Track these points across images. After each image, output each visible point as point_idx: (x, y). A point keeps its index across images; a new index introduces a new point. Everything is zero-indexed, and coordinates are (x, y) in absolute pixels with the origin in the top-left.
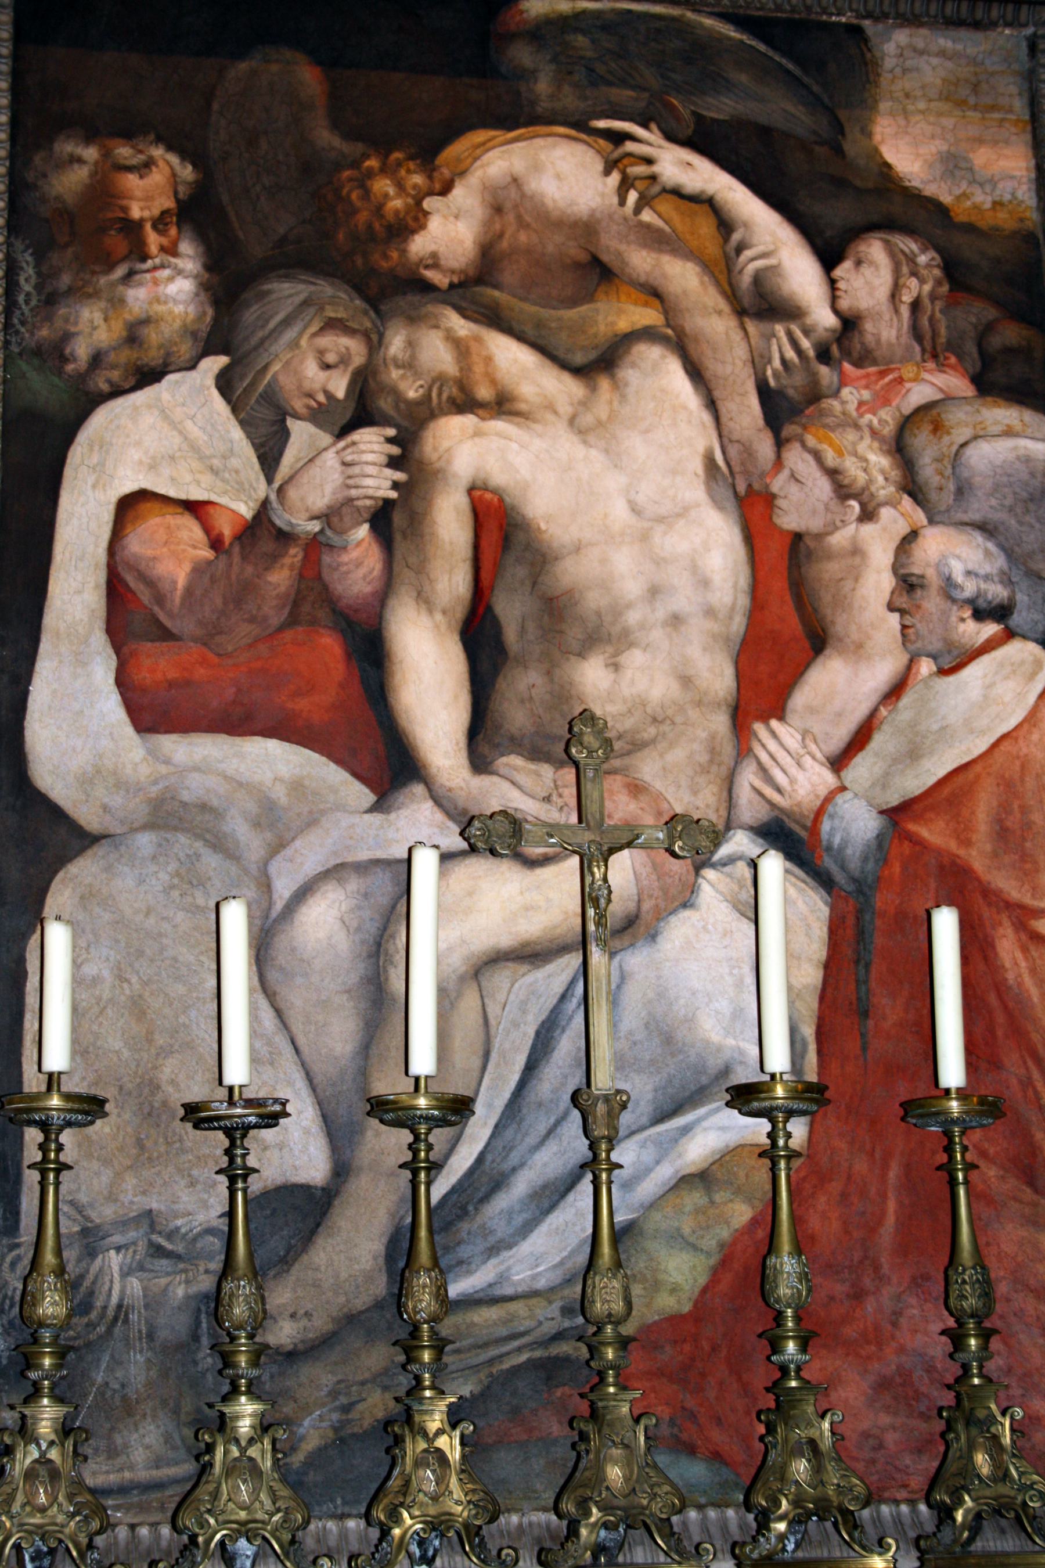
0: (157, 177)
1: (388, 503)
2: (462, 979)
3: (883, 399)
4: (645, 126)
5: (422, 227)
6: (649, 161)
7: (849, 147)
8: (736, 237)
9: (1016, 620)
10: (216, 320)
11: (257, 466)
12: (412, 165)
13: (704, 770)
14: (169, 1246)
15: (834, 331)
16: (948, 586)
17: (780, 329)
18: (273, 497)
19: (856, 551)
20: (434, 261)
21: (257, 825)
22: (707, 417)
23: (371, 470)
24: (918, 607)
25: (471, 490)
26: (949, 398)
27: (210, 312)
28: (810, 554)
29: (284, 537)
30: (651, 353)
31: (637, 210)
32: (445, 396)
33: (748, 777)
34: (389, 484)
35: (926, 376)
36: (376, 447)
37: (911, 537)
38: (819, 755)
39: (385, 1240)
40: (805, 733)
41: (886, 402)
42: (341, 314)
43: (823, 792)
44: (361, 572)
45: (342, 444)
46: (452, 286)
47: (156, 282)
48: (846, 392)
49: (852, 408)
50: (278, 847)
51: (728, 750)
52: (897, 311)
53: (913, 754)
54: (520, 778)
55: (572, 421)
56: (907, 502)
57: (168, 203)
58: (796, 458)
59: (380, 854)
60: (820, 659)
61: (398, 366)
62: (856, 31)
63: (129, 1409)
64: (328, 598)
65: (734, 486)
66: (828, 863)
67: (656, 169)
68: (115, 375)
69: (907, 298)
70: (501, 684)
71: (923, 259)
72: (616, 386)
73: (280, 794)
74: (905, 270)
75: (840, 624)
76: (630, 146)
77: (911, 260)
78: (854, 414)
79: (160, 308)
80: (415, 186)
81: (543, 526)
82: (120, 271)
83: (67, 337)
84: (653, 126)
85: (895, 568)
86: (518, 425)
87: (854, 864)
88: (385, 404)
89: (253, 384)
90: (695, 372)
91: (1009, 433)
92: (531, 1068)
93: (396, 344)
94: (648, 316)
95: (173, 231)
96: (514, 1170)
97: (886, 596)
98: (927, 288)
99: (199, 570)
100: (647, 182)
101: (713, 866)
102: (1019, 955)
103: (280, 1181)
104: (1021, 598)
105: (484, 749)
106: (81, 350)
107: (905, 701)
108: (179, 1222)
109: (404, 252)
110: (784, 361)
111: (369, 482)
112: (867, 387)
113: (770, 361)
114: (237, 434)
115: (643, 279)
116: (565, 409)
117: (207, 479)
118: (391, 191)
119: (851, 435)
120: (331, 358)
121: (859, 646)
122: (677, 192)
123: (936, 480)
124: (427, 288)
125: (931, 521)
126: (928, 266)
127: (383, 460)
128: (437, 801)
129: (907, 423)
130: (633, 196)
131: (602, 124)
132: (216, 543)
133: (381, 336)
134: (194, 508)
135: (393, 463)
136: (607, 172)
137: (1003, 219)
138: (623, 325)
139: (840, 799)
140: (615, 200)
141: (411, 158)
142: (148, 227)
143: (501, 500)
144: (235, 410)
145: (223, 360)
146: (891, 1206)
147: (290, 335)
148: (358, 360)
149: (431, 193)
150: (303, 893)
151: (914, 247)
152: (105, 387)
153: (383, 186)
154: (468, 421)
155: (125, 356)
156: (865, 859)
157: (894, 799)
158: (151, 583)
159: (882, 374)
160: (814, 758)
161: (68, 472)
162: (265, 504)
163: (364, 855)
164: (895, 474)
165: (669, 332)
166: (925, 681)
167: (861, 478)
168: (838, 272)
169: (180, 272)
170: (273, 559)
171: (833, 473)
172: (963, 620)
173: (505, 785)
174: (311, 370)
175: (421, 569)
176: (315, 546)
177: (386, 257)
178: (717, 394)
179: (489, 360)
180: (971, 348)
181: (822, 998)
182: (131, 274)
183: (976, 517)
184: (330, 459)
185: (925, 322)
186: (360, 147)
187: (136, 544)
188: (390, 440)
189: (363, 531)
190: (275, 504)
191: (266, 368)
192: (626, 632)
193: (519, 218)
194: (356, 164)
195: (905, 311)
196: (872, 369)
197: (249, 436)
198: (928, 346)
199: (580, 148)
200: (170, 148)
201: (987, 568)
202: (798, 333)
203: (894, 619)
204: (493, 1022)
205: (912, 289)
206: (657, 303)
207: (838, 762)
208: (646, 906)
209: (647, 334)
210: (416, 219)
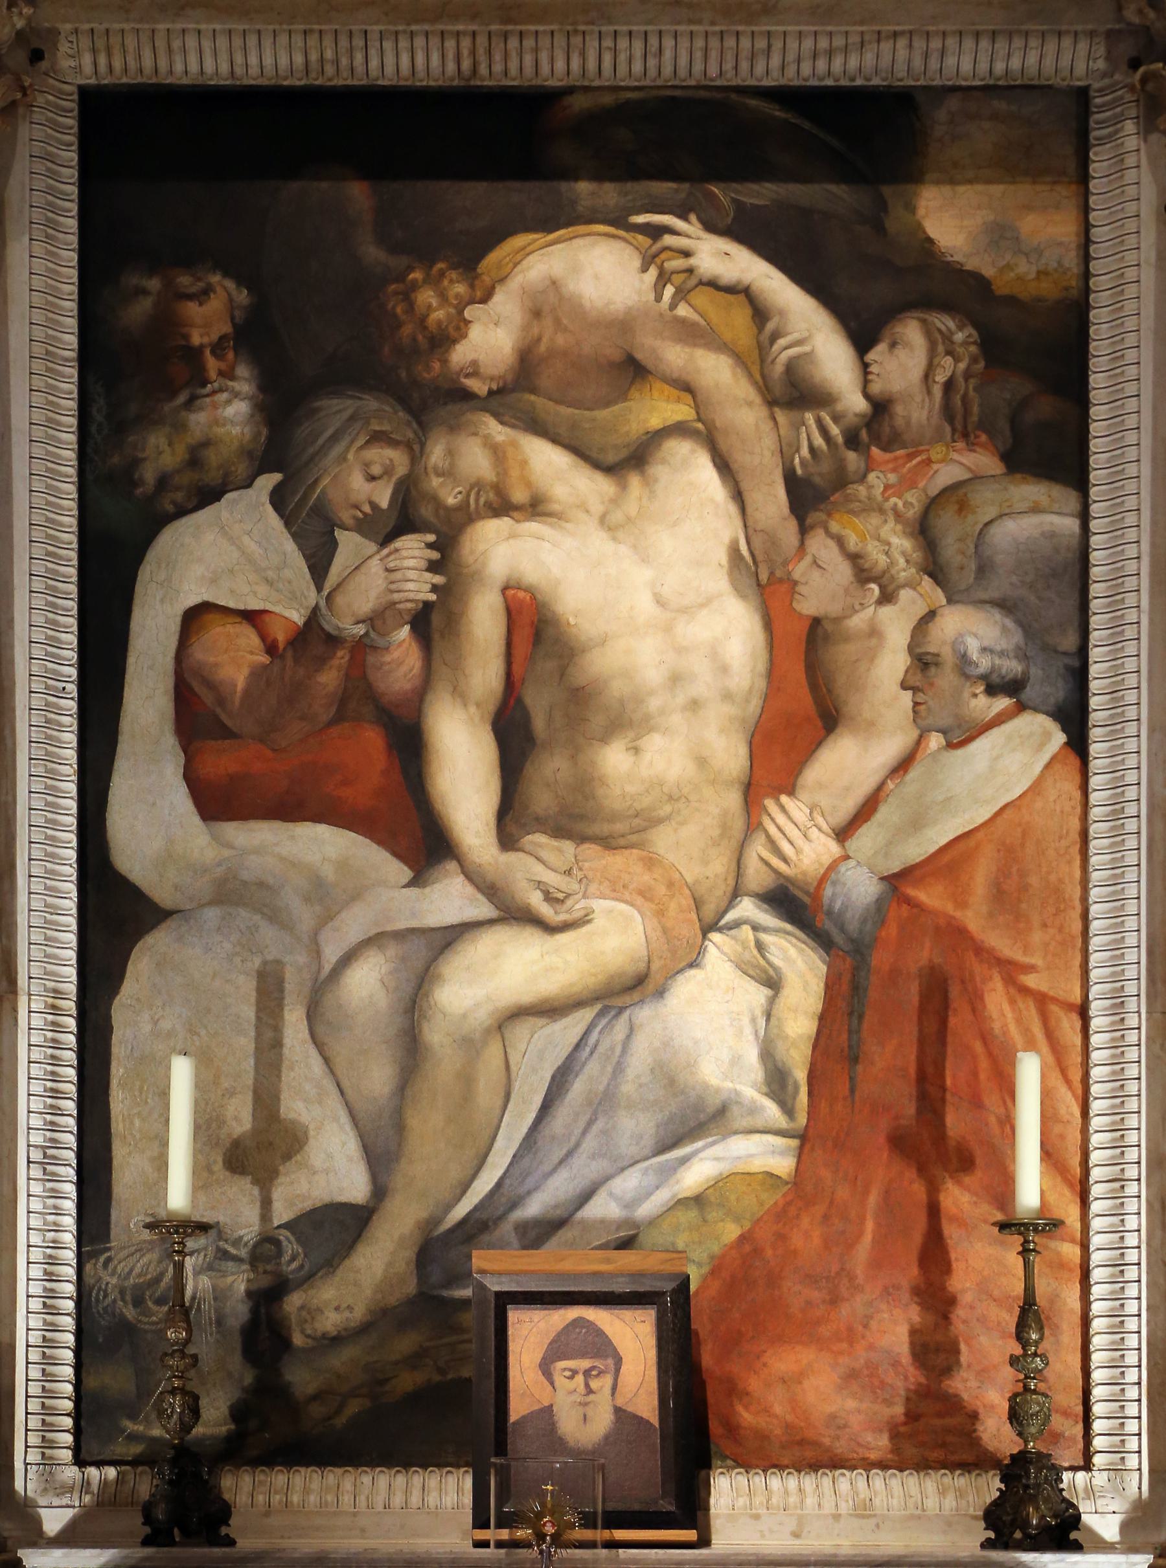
0: (216, 304)
1: (427, 606)
2: (488, 1031)
3: (909, 482)
4: (684, 217)
5: (464, 336)
6: (687, 254)
7: (891, 225)
8: (770, 326)
9: (1028, 694)
10: (270, 439)
11: (308, 576)
13: (716, 843)
14: (233, 1251)
15: (863, 416)
16: (964, 660)
17: (810, 417)
18: (323, 603)
19: (874, 632)
20: (474, 370)
21: (307, 900)
22: (733, 509)
23: (412, 574)
24: (932, 685)
25: (505, 589)
26: (977, 478)
27: (265, 432)
28: (827, 637)
29: (333, 641)
30: (680, 449)
31: (673, 306)
32: (482, 500)
33: (758, 848)
34: (428, 587)
35: (955, 456)
36: (417, 553)
37: (931, 615)
38: (825, 827)
39: (416, 1249)
41: (913, 485)
42: (386, 427)
43: (827, 861)
44: (404, 669)
45: (385, 551)
46: (491, 393)
47: (215, 406)
48: (872, 477)
50: (327, 918)
51: (739, 824)
52: (929, 392)
53: (916, 823)
54: (544, 854)
55: (603, 520)
56: (927, 581)
57: (227, 328)
58: (820, 546)
59: (414, 924)
60: (832, 737)
61: (438, 475)
64: (370, 695)
66: (828, 925)
68: (179, 496)
69: (941, 377)
70: (529, 769)
71: (959, 337)
72: (648, 482)
73: (328, 872)
74: (941, 348)
76: (668, 240)
77: (947, 338)
78: (880, 498)
79: (220, 431)
80: (457, 296)
81: (572, 621)
82: (182, 398)
83: (136, 463)
84: (693, 217)
85: (911, 648)
86: (551, 525)
87: (853, 926)
88: (426, 512)
89: (305, 497)
90: (723, 466)
91: (1036, 509)
92: (546, 1107)
93: (436, 454)
94: (681, 412)
95: (231, 355)
96: (529, 1193)
97: (901, 675)
98: (962, 366)
99: (258, 673)
100: (683, 276)
101: (720, 930)
102: (1006, 1007)
103: (327, 1199)
104: (1035, 672)
105: (512, 828)
106: (149, 474)
107: (914, 773)
108: (242, 1233)
109: (445, 362)
110: (812, 449)
111: (411, 586)
112: (894, 470)
113: (798, 450)
114: (290, 546)
115: (675, 376)
116: (597, 508)
117: (262, 589)
118: (434, 302)
119: (875, 520)
120: (376, 470)
121: (872, 724)
122: (713, 284)
123: (958, 559)
124: (467, 396)
125: (950, 601)
126: (965, 343)
127: (423, 564)
129: (933, 504)
130: (669, 291)
131: (641, 219)
132: (271, 649)
133: (423, 445)
134: (251, 617)
135: (433, 567)
136: (644, 269)
139: (843, 868)
140: (652, 296)
141: (454, 267)
142: (208, 352)
143: (533, 598)
144: (288, 524)
145: (277, 477)
146: (870, 1225)
148: (401, 470)
149: (472, 302)
150: (348, 959)
151: (951, 324)
152: (170, 508)
153: (426, 297)
154: (502, 524)
155: (186, 478)
156: (864, 921)
157: (895, 867)
159: (910, 457)
160: (820, 829)
161: (139, 589)
162: (315, 610)
163: (401, 925)
164: (917, 556)
165: (700, 426)
166: (934, 755)
167: (883, 560)
168: (871, 356)
169: (236, 395)
170: (321, 662)
171: (854, 557)
172: (975, 695)
173: (531, 860)
174: (358, 484)
175: (457, 666)
176: (362, 648)
177: (428, 368)
178: (744, 486)
179: (524, 463)
180: (1003, 424)
181: (815, 1047)
182: (193, 399)
183: (995, 594)
184: (375, 566)
186: (404, 260)
188: (430, 546)
189: (405, 632)
190: (324, 609)
191: (316, 482)
192: (647, 718)
193: (557, 322)
194: (401, 278)
195: (938, 392)
197: (301, 548)
198: (959, 427)
199: (618, 245)
200: (226, 274)
201: (1003, 644)
202: (828, 420)
204: (513, 1068)
205: (946, 367)
206: (688, 398)
207: (843, 834)
208: (655, 966)
209: (679, 430)
210: (458, 328)
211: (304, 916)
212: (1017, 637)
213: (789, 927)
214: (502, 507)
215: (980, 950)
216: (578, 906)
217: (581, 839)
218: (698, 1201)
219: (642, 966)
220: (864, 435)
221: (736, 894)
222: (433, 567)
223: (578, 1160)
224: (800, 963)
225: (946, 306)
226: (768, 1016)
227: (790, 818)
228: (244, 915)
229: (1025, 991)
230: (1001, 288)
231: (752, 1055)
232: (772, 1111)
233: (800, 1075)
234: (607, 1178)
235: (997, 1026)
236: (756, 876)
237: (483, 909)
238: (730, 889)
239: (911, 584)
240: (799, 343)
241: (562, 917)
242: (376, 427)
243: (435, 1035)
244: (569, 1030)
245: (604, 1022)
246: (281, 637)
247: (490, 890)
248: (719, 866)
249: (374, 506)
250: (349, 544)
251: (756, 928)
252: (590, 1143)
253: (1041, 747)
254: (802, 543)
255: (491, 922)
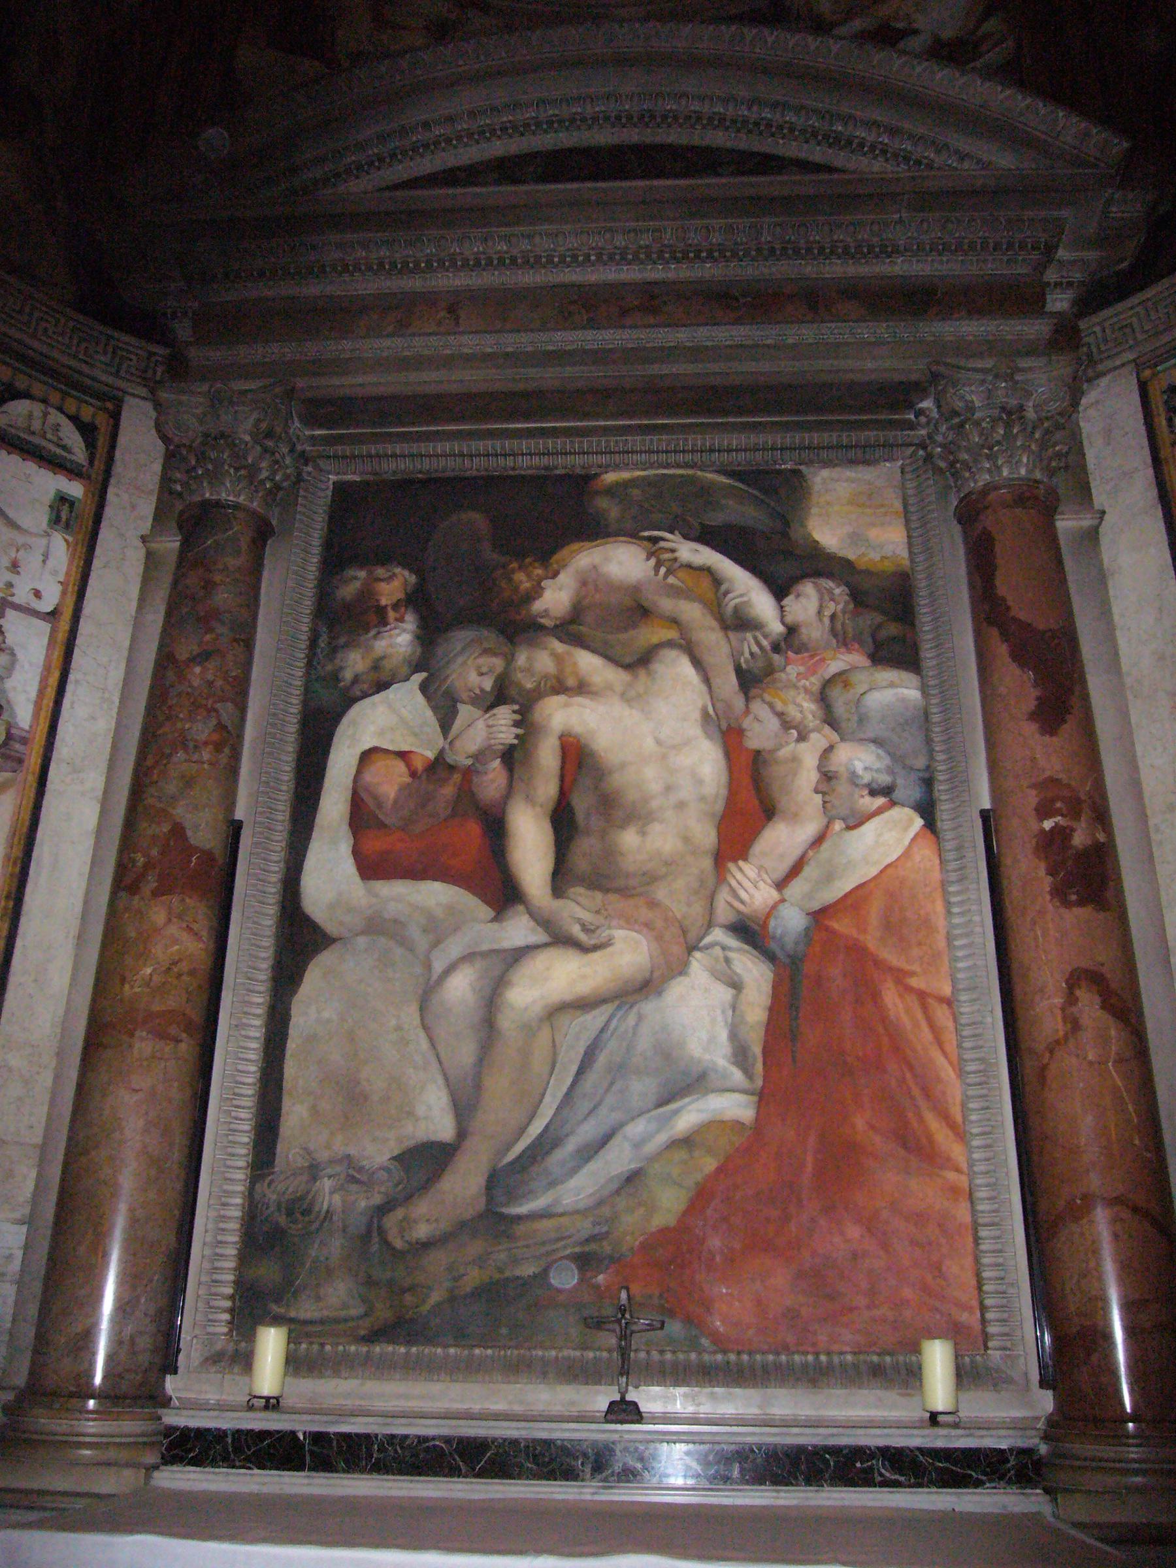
0: (396, 583)
2: (541, 1020)
3: (812, 671)
4: (672, 532)
5: (540, 596)
6: (673, 551)
7: (792, 534)
8: (723, 588)
9: (898, 794)
10: (423, 653)
11: (439, 730)
12: (536, 564)
13: (696, 892)
15: (781, 634)
16: (853, 778)
17: (749, 636)
18: (447, 747)
19: (795, 759)
22: (704, 688)
23: (504, 729)
24: (834, 790)
25: (561, 737)
26: (854, 668)
27: (419, 650)
29: (452, 768)
30: (671, 654)
31: (666, 576)
32: (549, 684)
33: (723, 896)
35: (841, 656)
36: (508, 716)
37: (830, 749)
38: (769, 881)
39: (486, 1177)
40: (761, 868)
41: (814, 673)
43: (771, 902)
46: (556, 626)
47: (391, 637)
48: (789, 668)
49: (793, 676)
50: (436, 943)
51: (711, 881)
52: (821, 620)
53: (829, 877)
54: (580, 899)
55: (622, 695)
56: (827, 729)
57: (401, 595)
58: (758, 708)
59: (496, 947)
60: (770, 824)
62: (797, 473)
63: (329, 1272)
65: (719, 726)
66: (773, 946)
67: (677, 554)
68: (365, 687)
69: (827, 613)
71: (837, 591)
72: (649, 674)
73: (439, 913)
74: (826, 597)
75: (783, 802)
76: (662, 544)
77: (830, 592)
78: (794, 680)
79: (390, 650)
82: (373, 632)
84: (676, 532)
86: (591, 700)
88: (513, 692)
90: (697, 663)
91: (892, 685)
92: (581, 1072)
93: (522, 659)
94: (671, 634)
95: (403, 609)
96: (567, 1135)
97: (813, 785)
98: (840, 607)
99: (403, 788)
101: (700, 949)
102: (898, 1001)
103: (425, 1139)
106: (348, 675)
107: (825, 846)
108: (365, 1163)
110: (752, 654)
111: (502, 735)
112: (802, 665)
113: (742, 654)
114: (429, 713)
115: (668, 614)
116: (619, 688)
119: (792, 693)
120: (484, 670)
122: (689, 566)
124: (542, 628)
128: (532, 915)
129: (828, 683)
130: (663, 570)
131: (646, 534)
132: (413, 774)
133: (513, 655)
134: (403, 755)
135: (517, 724)
136: (648, 559)
137: (888, 567)
138: (655, 640)
139: (781, 907)
142: (389, 608)
143: (578, 741)
145: (424, 675)
146: (810, 1160)
147: (460, 660)
149: (547, 578)
152: (358, 693)
153: (520, 576)
154: (562, 698)
156: (796, 943)
157: (816, 906)
158: (376, 797)
159: (812, 657)
160: (765, 882)
162: (442, 751)
163: (485, 947)
164: (820, 713)
167: (798, 716)
168: (785, 602)
169: (404, 630)
170: (446, 780)
171: (780, 715)
173: (573, 905)
176: (468, 773)
178: (711, 675)
179: (575, 664)
181: (767, 1031)
182: (379, 633)
183: (872, 735)
184: (480, 724)
185: (839, 627)
186: (508, 558)
187: (369, 777)
188: (514, 712)
189: (497, 763)
191: (448, 677)
193: (596, 586)
195: (827, 621)
196: (806, 654)
197: (435, 714)
198: (841, 639)
201: (877, 765)
202: (760, 637)
203: (818, 798)
204: (557, 1043)
205: (831, 608)
207: (781, 885)
208: (657, 974)
210: (536, 592)
211: (422, 942)
212: (887, 761)
213: (746, 947)
214: (559, 687)
215: (877, 963)
216: (604, 934)
217: (607, 891)
218: (687, 1142)
219: (647, 975)
220: (783, 644)
221: (710, 925)
222: (517, 724)
223: (603, 1111)
224: (755, 972)
225: (830, 576)
226: (734, 1008)
227: (745, 875)
228: (383, 941)
229: (909, 989)
230: (862, 565)
231: (723, 1035)
232: (737, 1076)
233: (757, 1050)
234: (621, 1125)
235: (892, 1014)
236: (723, 914)
237: (540, 937)
238: (706, 923)
239: (817, 730)
240: (741, 596)
241: (593, 942)
242: (486, 645)
243: (506, 1022)
244: (594, 1020)
245: (620, 1014)
246: (419, 765)
247: (544, 922)
248: (697, 909)
249: (482, 690)
250: (465, 711)
251: (724, 948)
252: (610, 1100)
253: (906, 829)
254: (747, 707)
255: (546, 945)
